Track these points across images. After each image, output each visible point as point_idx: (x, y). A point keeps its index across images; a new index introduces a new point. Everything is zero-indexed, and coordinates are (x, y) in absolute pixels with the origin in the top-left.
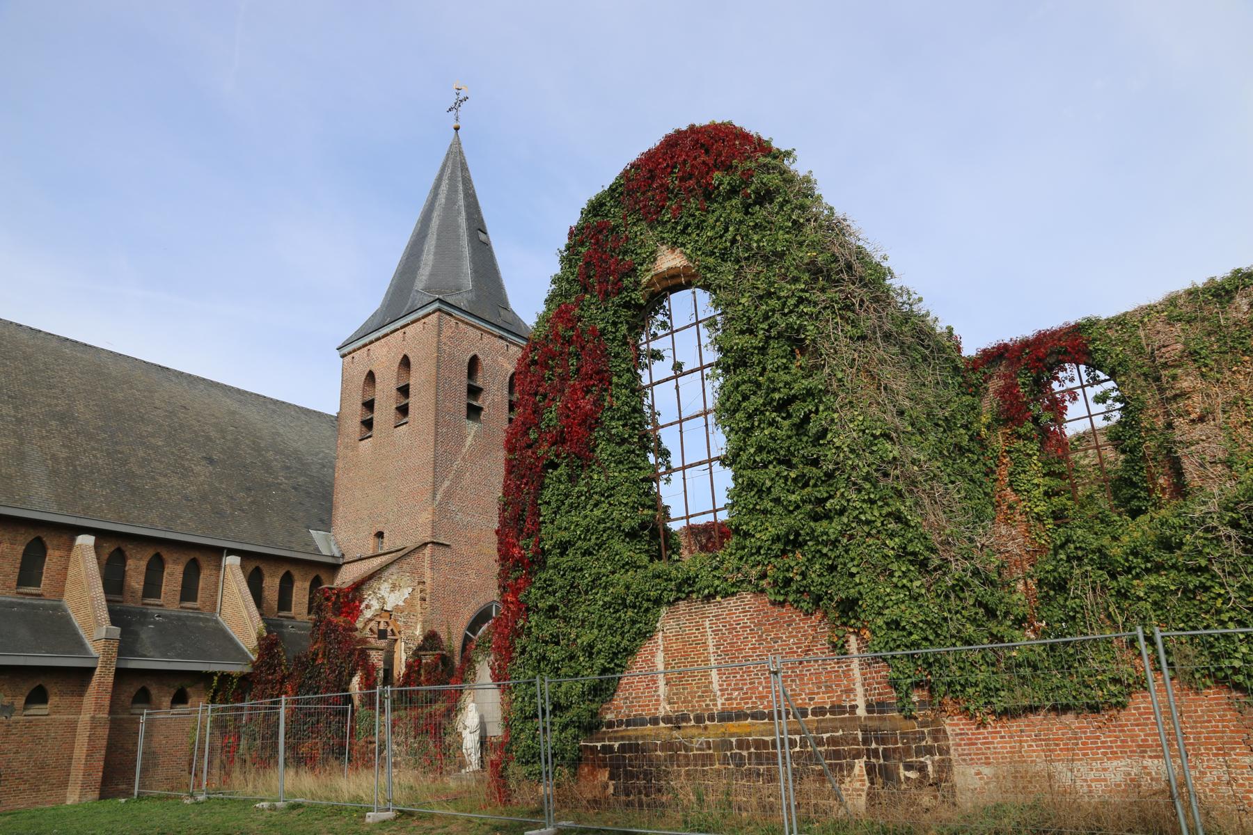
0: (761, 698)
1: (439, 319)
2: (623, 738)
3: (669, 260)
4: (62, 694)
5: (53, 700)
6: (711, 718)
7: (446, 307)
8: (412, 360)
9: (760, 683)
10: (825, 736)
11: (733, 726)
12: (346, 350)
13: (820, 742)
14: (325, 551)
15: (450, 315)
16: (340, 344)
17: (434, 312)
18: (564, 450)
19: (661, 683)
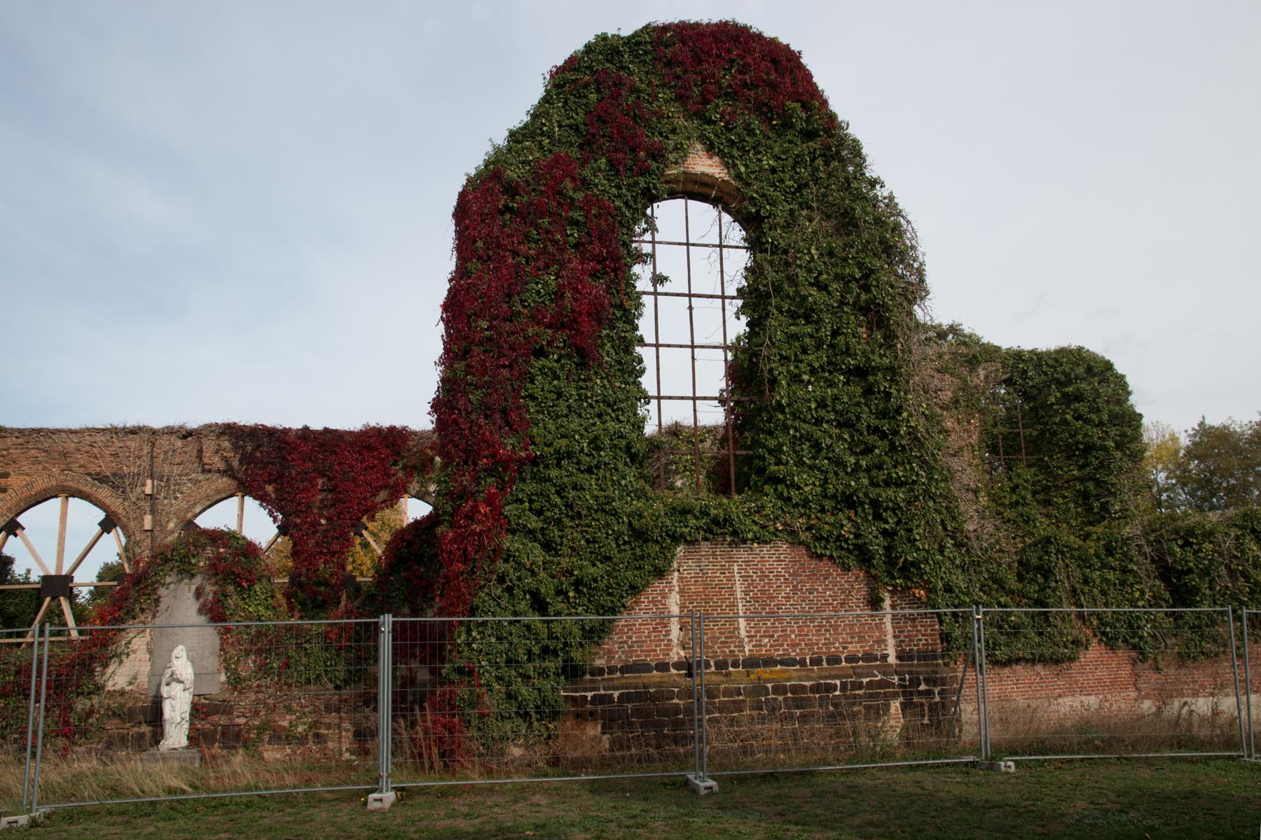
0: (794, 645)
3: (704, 164)
6: (735, 664)
10: (865, 680)
13: (860, 686)
18: (562, 336)
19: (675, 627)
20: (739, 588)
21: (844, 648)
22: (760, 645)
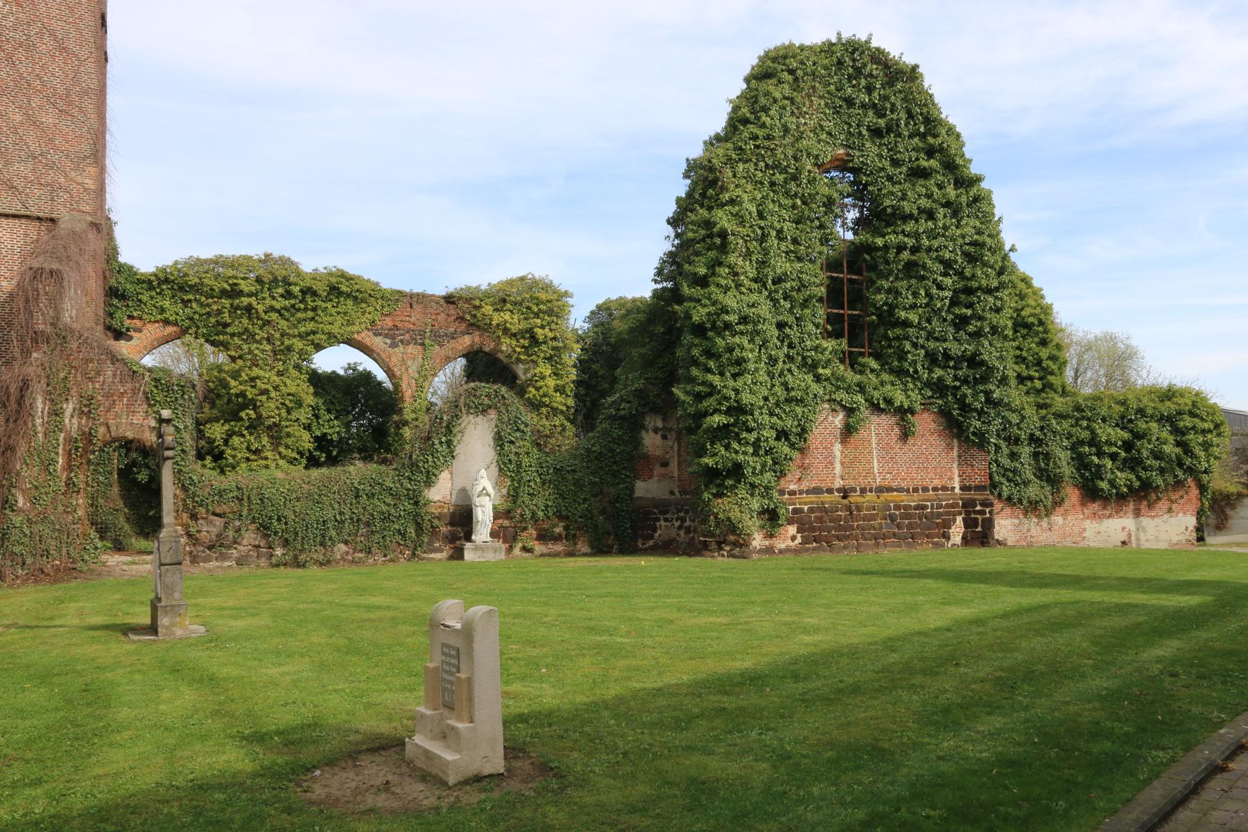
2: (811, 503)
6: (871, 491)
13: (940, 506)
20: (874, 441)
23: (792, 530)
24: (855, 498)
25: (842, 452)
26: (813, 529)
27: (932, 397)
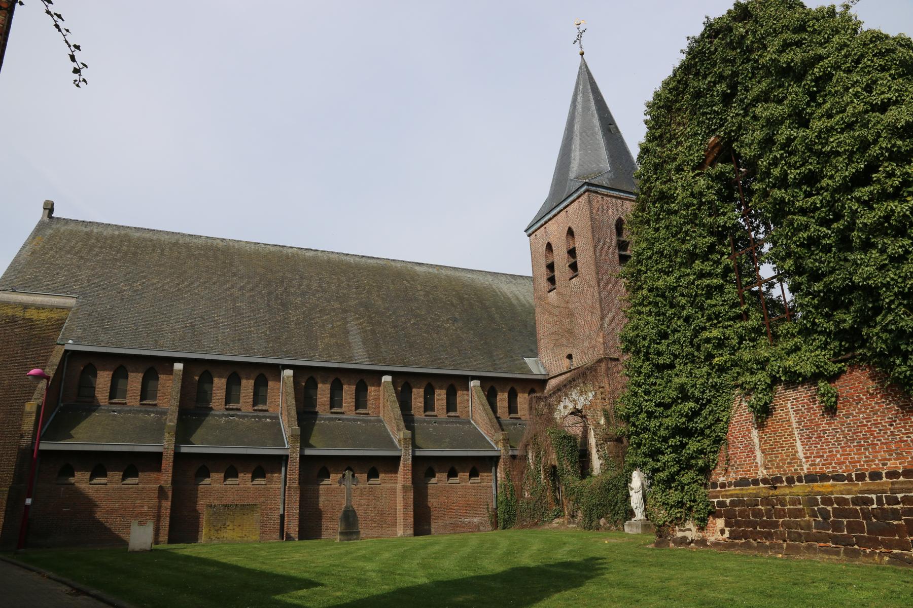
0: (840, 463)
1: (589, 197)
2: (732, 496)
4: (386, 472)
5: (382, 476)
6: (800, 480)
7: (591, 187)
8: (574, 230)
9: (838, 452)
10: (899, 496)
11: (817, 486)
12: (530, 231)
14: (535, 371)
15: (597, 193)
16: (526, 228)
17: (585, 192)
19: (758, 453)
20: (794, 420)
21: (884, 464)
22: (815, 465)
23: (720, 523)
24: (783, 490)
25: (761, 439)
26: (738, 524)
27: (851, 349)
